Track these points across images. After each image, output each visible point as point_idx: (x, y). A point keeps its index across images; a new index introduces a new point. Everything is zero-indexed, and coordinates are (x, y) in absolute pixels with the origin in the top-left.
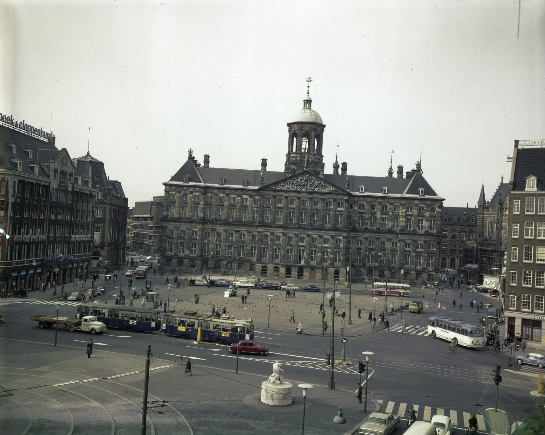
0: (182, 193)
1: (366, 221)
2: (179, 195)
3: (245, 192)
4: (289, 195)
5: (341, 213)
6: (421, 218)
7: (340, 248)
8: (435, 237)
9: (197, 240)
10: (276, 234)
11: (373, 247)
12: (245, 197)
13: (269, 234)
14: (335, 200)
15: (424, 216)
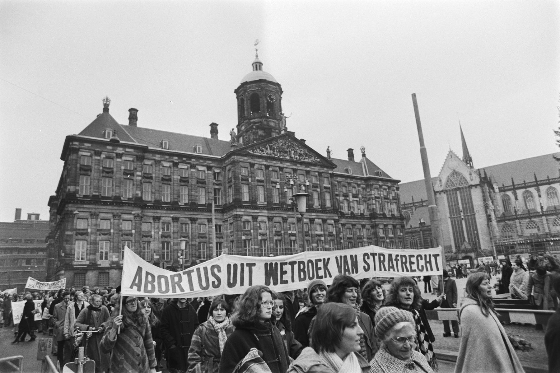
0: (103, 156)
1: (341, 204)
2: (98, 158)
3: (201, 161)
4: (271, 164)
5: (328, 190)
6: (386, 200)
7: (333, 235)
8: (400, 221)
9: (131, 234)
10: (260, 219)
11: (352, 236)
12: (201, 168)
13: (249, 218)
14: (320, 174)
15: (387, 199)
